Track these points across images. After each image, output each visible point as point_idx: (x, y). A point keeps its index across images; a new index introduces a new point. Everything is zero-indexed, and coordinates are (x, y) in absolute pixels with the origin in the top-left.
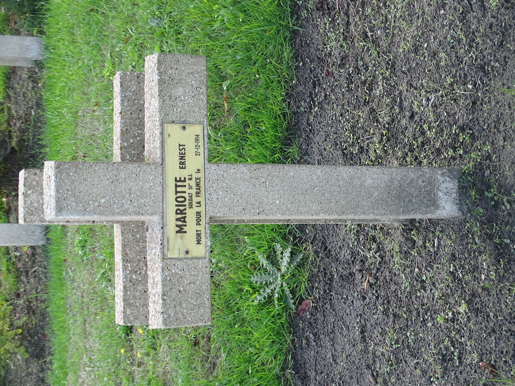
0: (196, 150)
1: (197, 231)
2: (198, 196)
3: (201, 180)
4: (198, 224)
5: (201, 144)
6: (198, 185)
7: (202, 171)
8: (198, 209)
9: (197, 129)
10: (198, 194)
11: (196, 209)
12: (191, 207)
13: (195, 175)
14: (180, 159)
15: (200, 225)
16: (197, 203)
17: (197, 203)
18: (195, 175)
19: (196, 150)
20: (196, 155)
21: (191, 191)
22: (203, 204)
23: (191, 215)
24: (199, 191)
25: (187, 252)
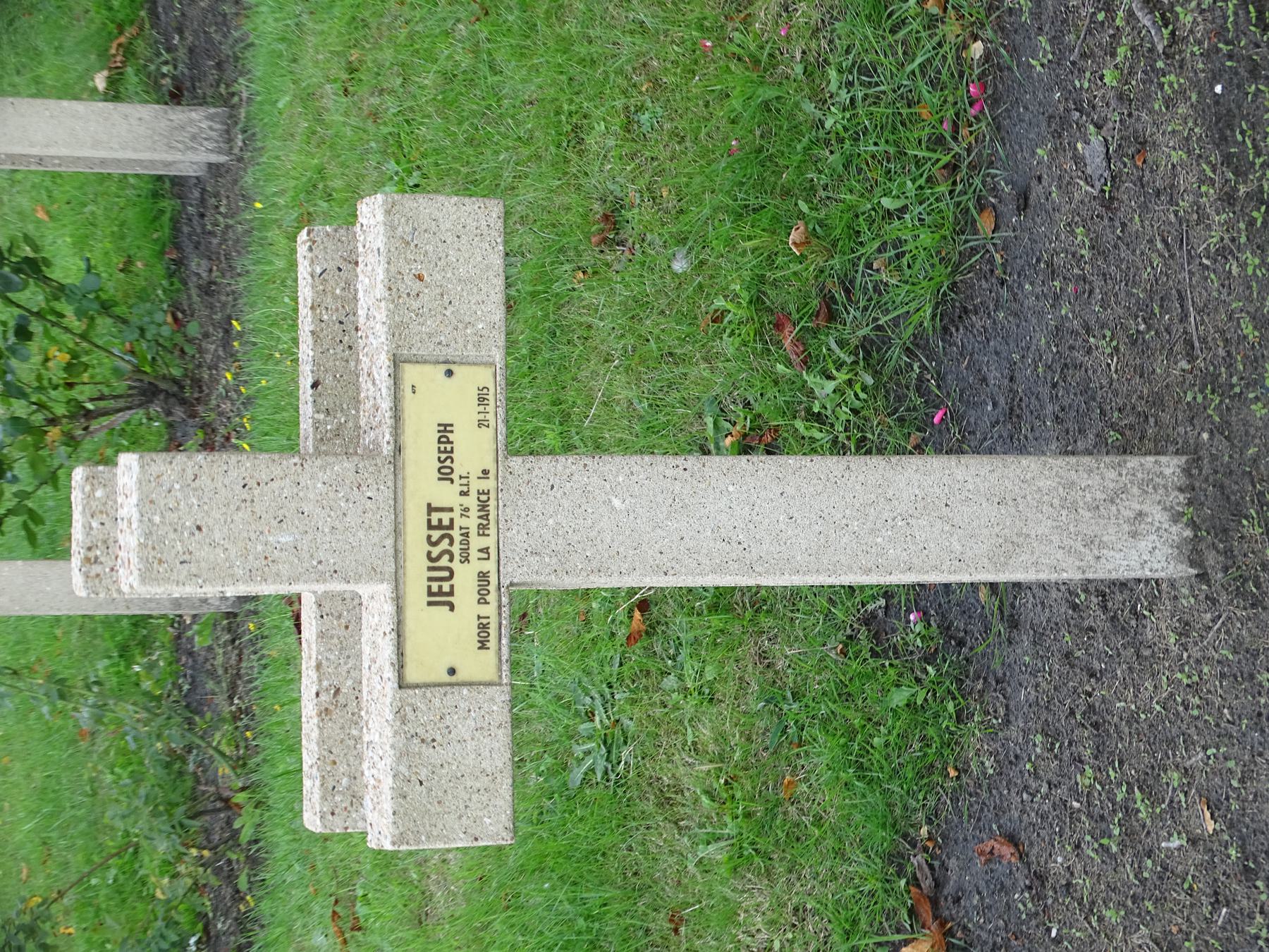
1: (479, 617)
2: (483, 535)
3: (492, 495)
4: (483, 601)
6: (483, 506)
9: (484, 377)
10: (483, 529)
11: (476, 566)
12: (466, 559)
13: (476, 485)
15: (487, 603)
16: (480, 551)
17: (480, 551)
18: (476, 485)
21: (463, 522)
22: (493, 552)
23: (465, 579)
24: (485, 522)
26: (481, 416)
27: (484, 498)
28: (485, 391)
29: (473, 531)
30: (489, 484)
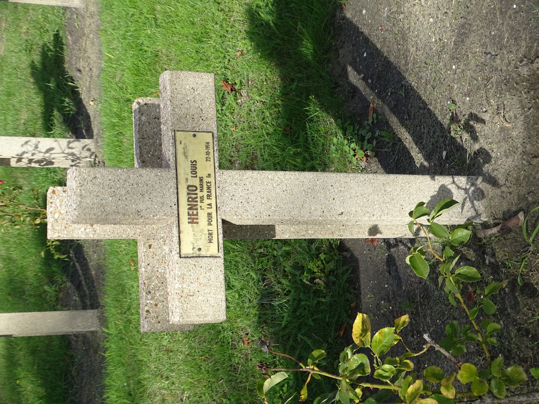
0: (207, 156)
1: (208, 230)
2: (209, 199)
3: (212, 184)
4: (210, 224)
5: (211, 151)
6: (209, 188)
7: (213, 175)
8: (210, 211)
15: (211, 225)
16: (208, 205)
17: (208, 205)
18: (205, 180)
19: (207, 156)
20: (207, 160)
25: (200, 249)
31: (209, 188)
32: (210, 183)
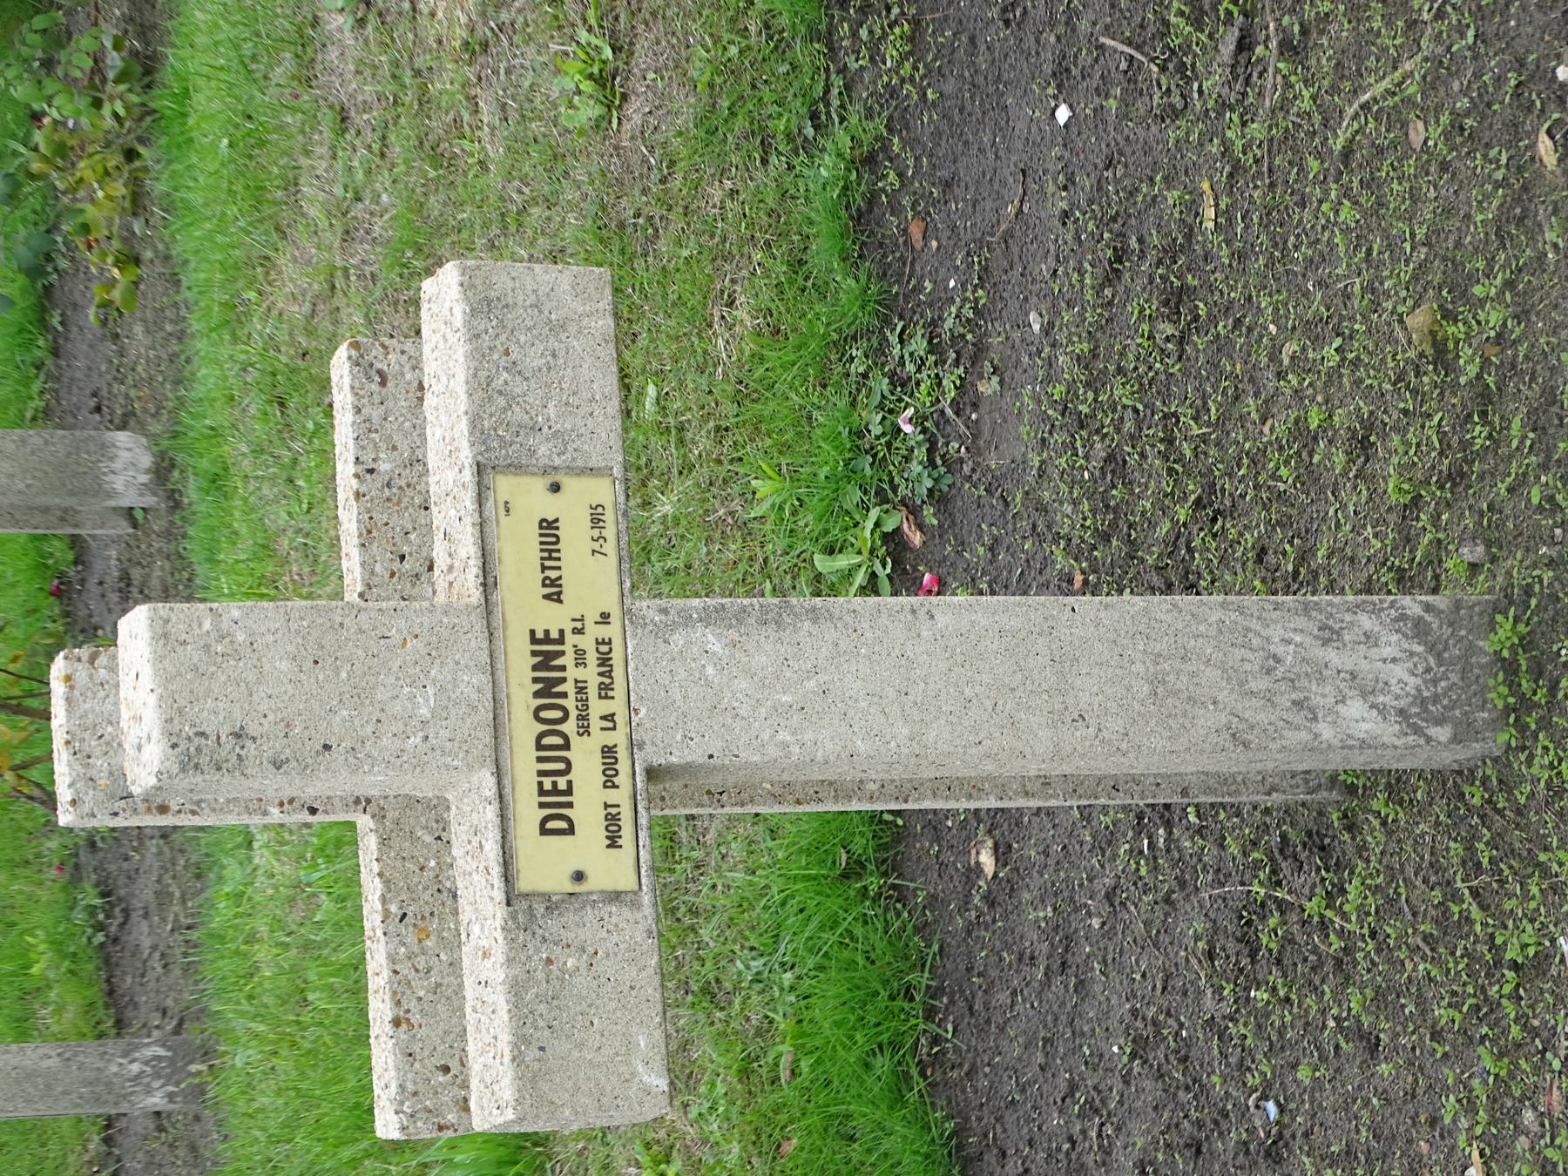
1: (606, 806)
2: (606, 697)
3: (614, 646)
4: (609, 784)
5: (610, 532)
6: (604, 661)
8: (609, 739)
11: (598, 738)
12: (584, 730)
14: (544, 585)
15: (615, 786)
16: (604, 718)
17: (604, 718)
18: (594, 631)
22: (621, 719)
24: (607, 681)
26: (596, 546)
27: (604, 648)
28: (600, 510)
29: (593, 692)
30: (612, 631)
31: (604, 661)
32: (610, 643)
